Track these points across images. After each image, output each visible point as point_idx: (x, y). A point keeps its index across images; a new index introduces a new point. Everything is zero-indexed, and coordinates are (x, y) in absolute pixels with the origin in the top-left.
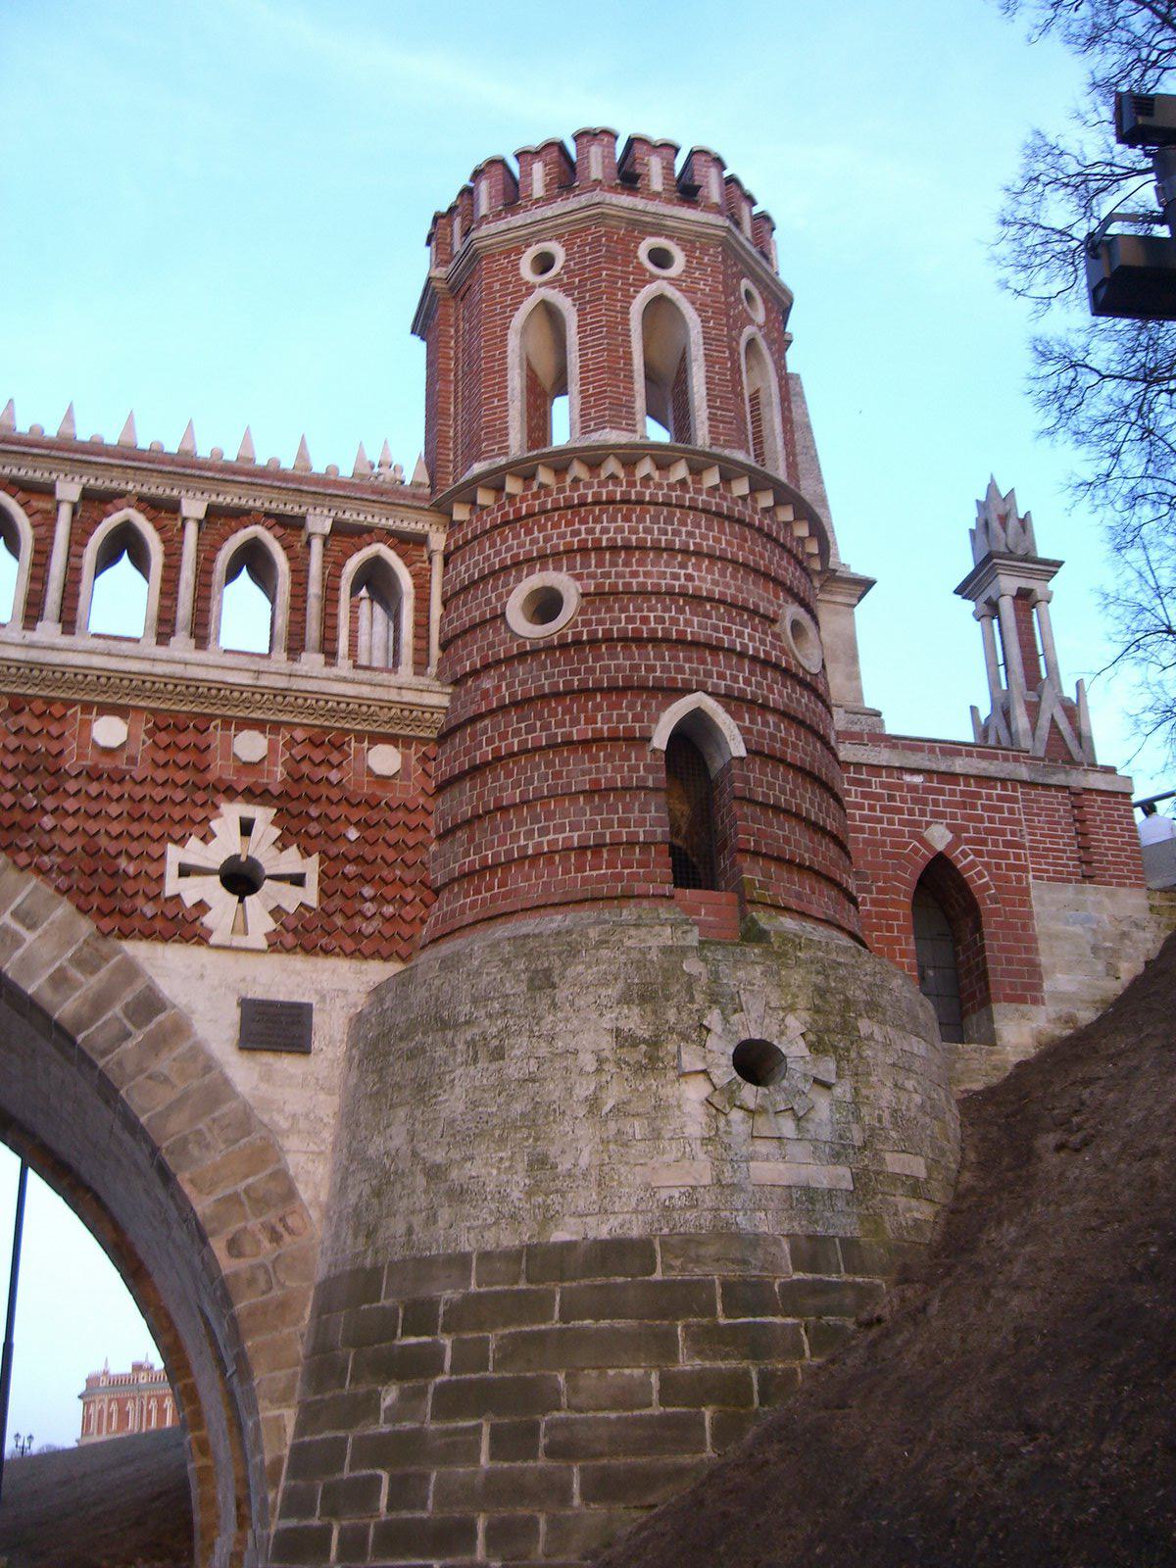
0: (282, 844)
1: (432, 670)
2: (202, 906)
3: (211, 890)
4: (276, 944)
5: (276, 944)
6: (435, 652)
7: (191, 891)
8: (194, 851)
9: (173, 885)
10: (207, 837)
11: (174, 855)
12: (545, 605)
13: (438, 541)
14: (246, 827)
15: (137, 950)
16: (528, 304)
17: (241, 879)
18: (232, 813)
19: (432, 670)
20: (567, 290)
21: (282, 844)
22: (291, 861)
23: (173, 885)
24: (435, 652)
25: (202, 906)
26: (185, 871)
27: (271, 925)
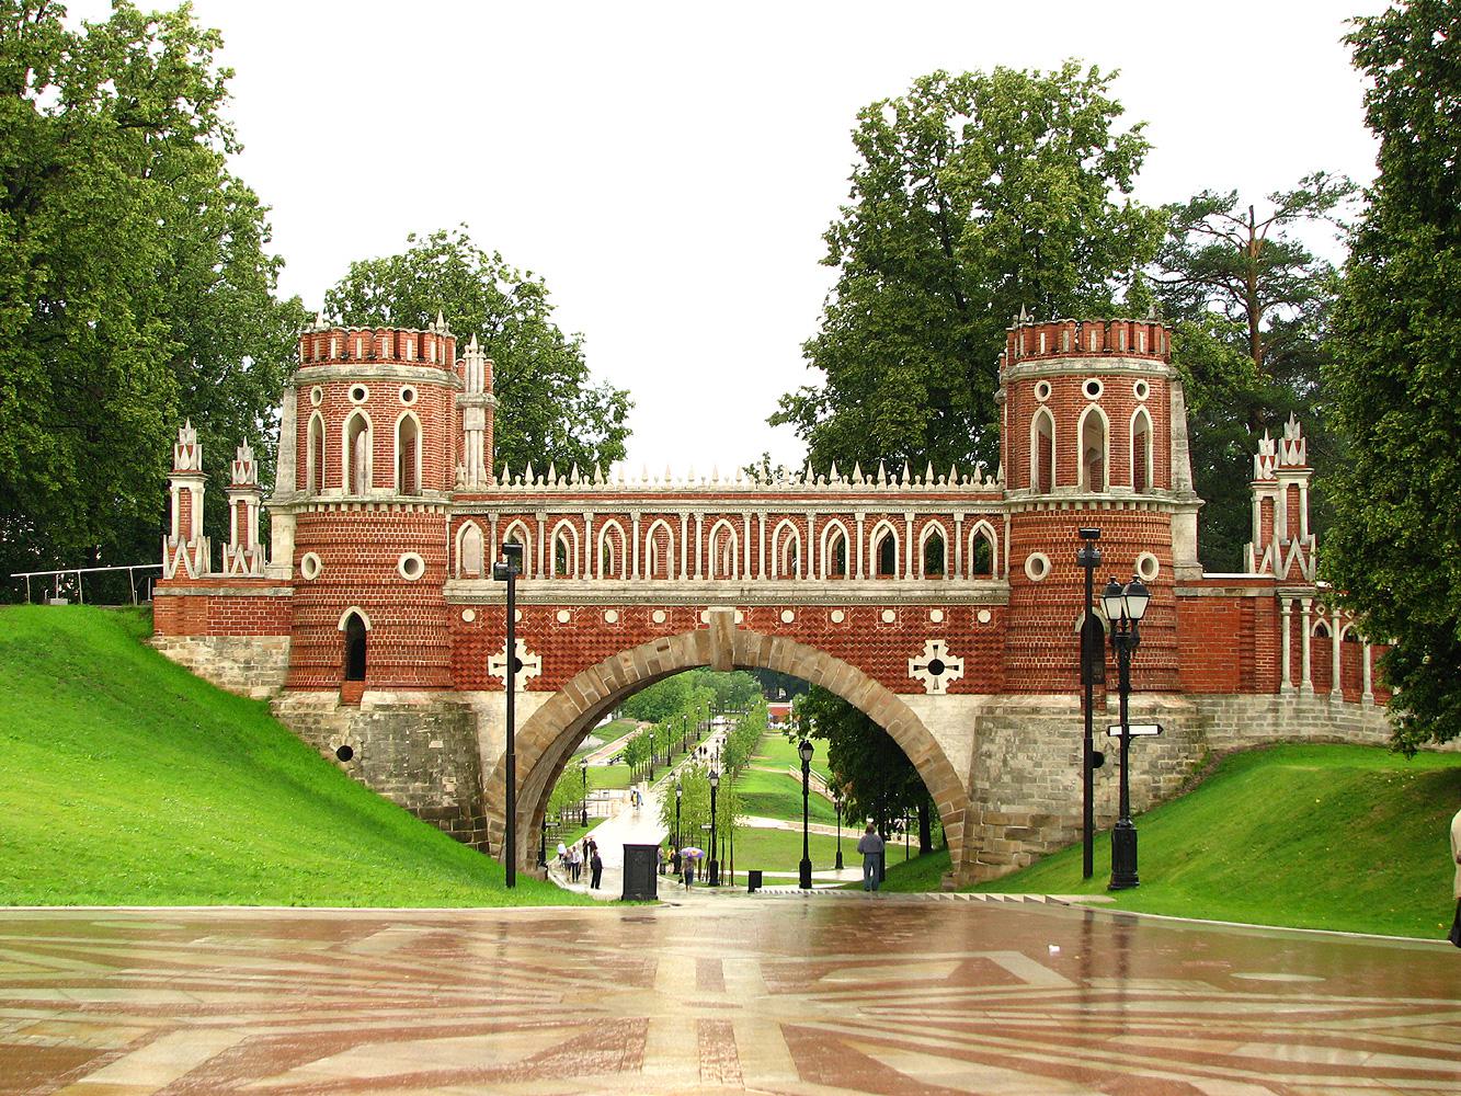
0: (949, 654)
1: (1006, 576)
2: (923, 680)
3: (925, 674)
4: (949, 691)
5: (949, 691)
6: (1007, 569)
7: (919, 675)
8: (919, 661)
9: (912, 673)
10: (923, 655)
11: (912, 663)
12: (1038, 565)
13: (1007, 518)
14: (936, 647)
15: (903, 698)
16: (1037, 414)
17: (936, 668)
18: (930, 643)
19: (1006, 576)
20: (1052, 407)
21: (949, 654)
22: (953, 661)
23: (912, 673)
24: (1007, 569)
25: (923, 680)
26: (916, 668)
27: (947, 685)
